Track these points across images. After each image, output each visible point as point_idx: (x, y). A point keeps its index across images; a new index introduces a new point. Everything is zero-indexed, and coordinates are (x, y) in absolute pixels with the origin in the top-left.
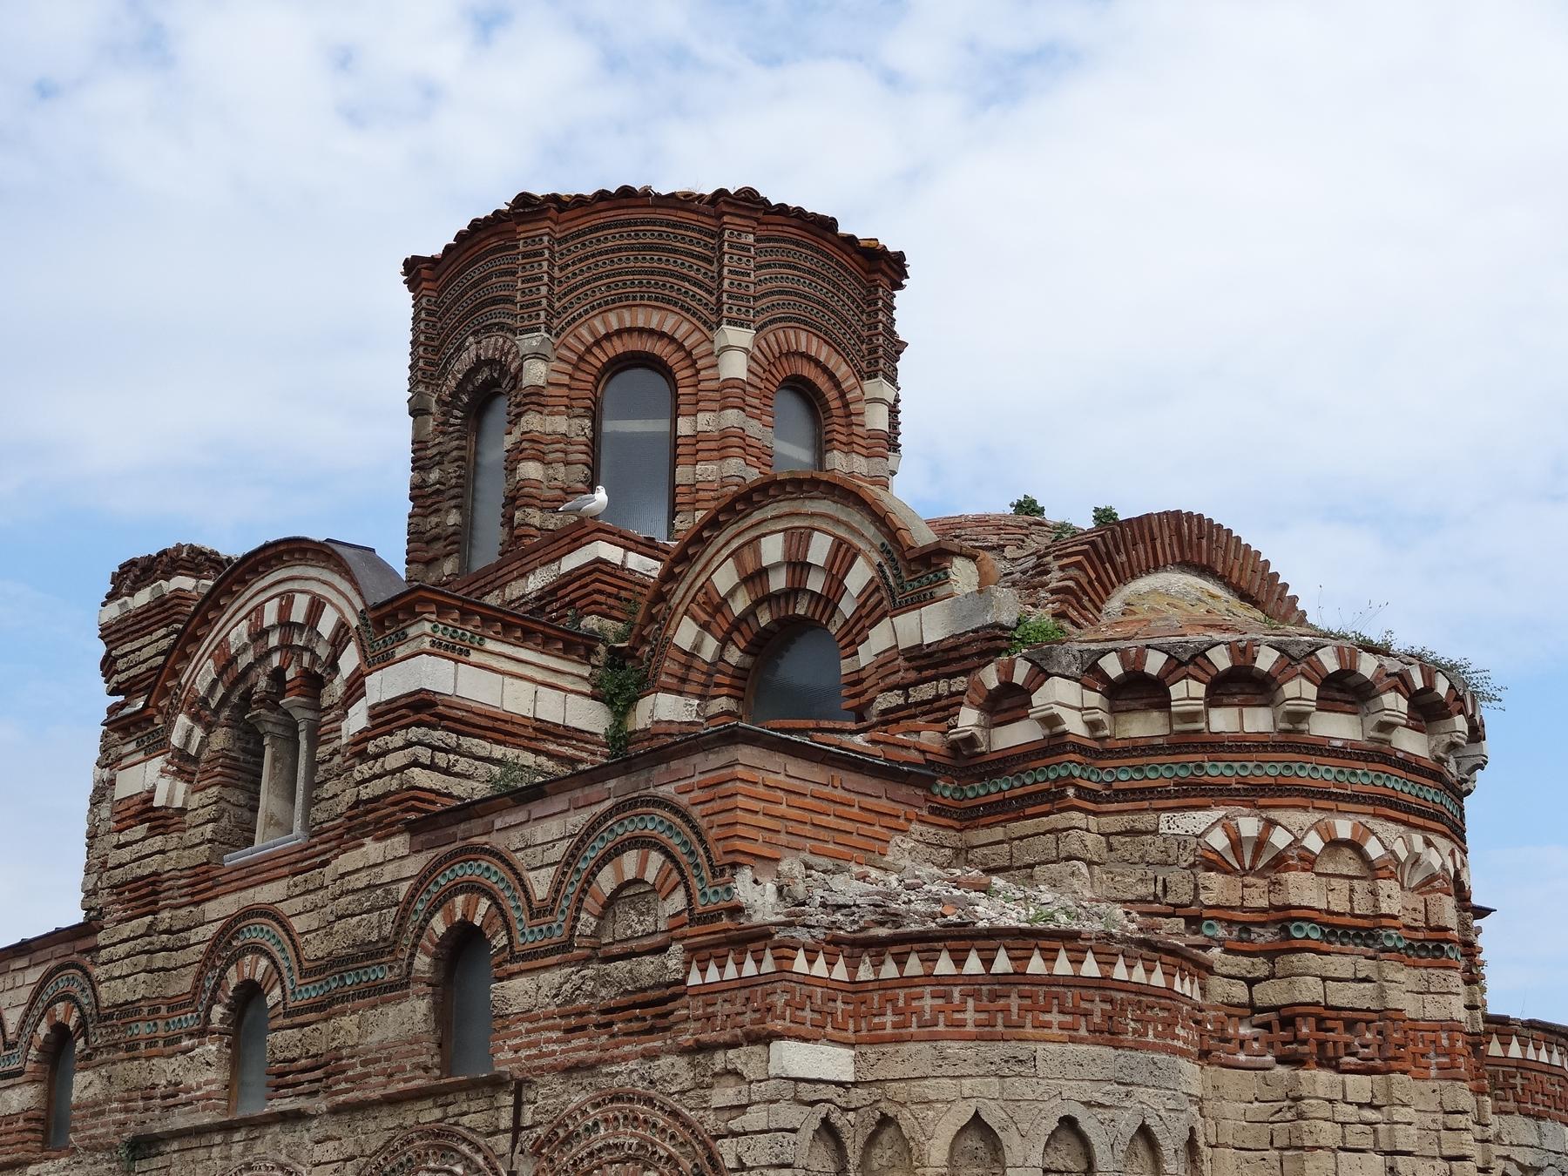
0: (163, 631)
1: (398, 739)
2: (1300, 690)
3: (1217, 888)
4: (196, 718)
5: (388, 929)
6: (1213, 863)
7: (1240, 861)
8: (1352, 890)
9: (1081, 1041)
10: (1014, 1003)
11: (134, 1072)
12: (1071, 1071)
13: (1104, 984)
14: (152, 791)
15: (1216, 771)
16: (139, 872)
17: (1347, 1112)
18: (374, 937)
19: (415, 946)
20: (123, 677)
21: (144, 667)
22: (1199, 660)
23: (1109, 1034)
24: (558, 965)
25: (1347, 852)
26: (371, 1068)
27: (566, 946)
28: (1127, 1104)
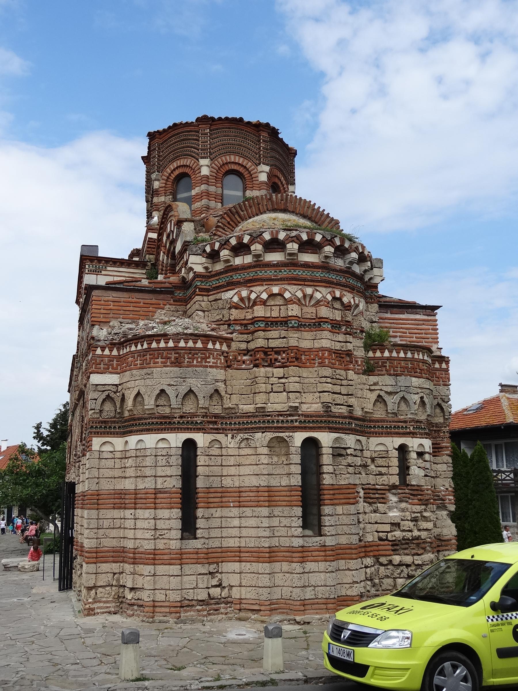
2: (257, 248)
3: (235, 314)
6: (236, 307)
7: (245, 305)
8: (280, 309)
9: (168, 366)
10: (148, 356)
12: (164, 376)
13: (176, 349)
15: (237, 277)
17: (274, 380)
22: (227, 243)
23: (177, 363)
25: (279, 297)
28: (184, 384)
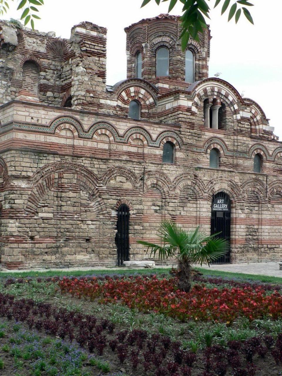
0: (103, 46)
1: (247, 123)
4: (199, 98)
5: (248, 150)
11: (194, 156)
14: (191, 107)
16: (190, 121)
18: (245, 150)
19: (252, 154)
20: (89, 49)
21: (96, 51)
24: (273, 163)
26: (245, 168)
27: (274, 161)
